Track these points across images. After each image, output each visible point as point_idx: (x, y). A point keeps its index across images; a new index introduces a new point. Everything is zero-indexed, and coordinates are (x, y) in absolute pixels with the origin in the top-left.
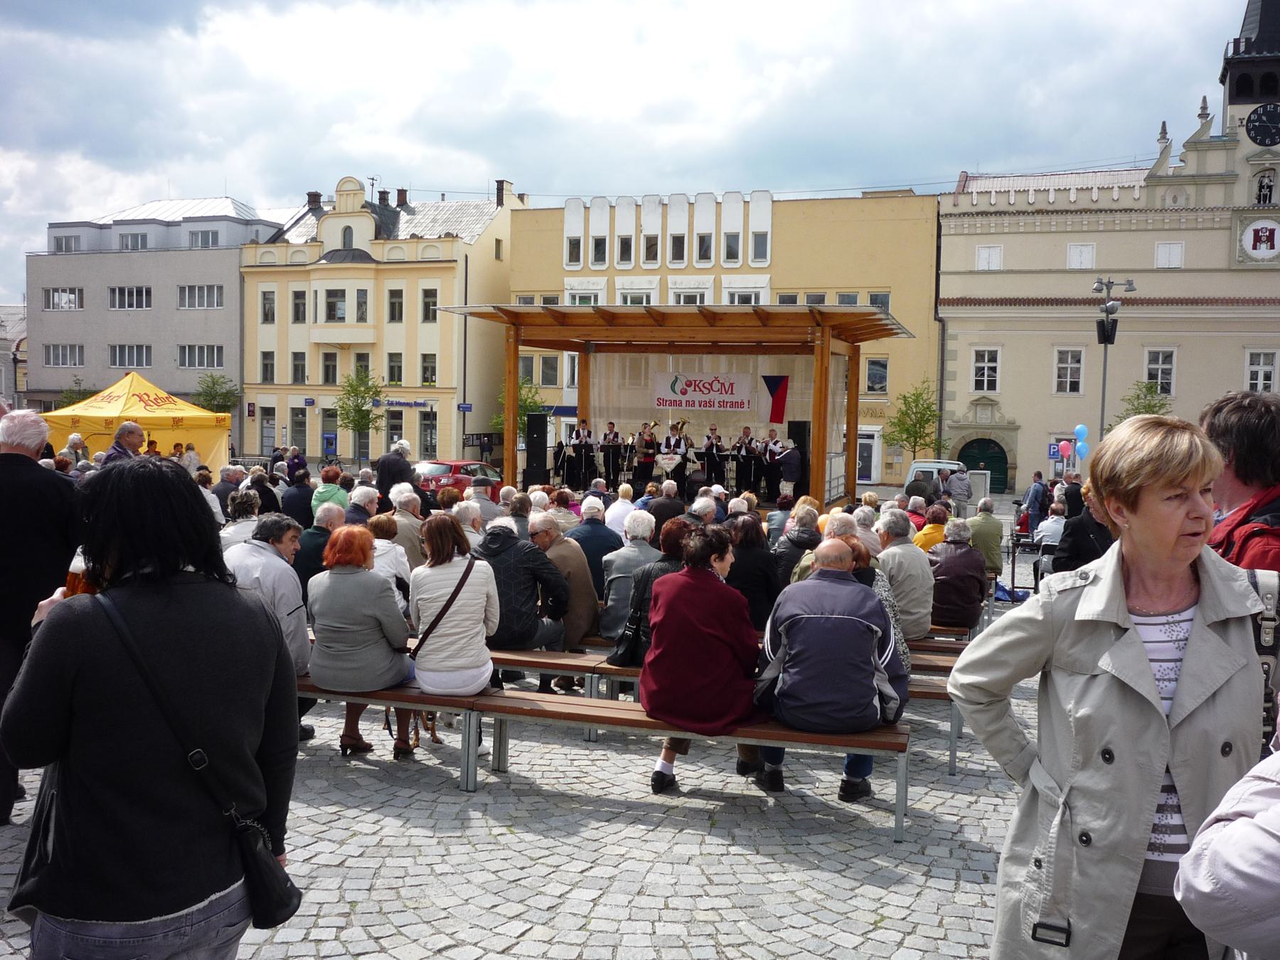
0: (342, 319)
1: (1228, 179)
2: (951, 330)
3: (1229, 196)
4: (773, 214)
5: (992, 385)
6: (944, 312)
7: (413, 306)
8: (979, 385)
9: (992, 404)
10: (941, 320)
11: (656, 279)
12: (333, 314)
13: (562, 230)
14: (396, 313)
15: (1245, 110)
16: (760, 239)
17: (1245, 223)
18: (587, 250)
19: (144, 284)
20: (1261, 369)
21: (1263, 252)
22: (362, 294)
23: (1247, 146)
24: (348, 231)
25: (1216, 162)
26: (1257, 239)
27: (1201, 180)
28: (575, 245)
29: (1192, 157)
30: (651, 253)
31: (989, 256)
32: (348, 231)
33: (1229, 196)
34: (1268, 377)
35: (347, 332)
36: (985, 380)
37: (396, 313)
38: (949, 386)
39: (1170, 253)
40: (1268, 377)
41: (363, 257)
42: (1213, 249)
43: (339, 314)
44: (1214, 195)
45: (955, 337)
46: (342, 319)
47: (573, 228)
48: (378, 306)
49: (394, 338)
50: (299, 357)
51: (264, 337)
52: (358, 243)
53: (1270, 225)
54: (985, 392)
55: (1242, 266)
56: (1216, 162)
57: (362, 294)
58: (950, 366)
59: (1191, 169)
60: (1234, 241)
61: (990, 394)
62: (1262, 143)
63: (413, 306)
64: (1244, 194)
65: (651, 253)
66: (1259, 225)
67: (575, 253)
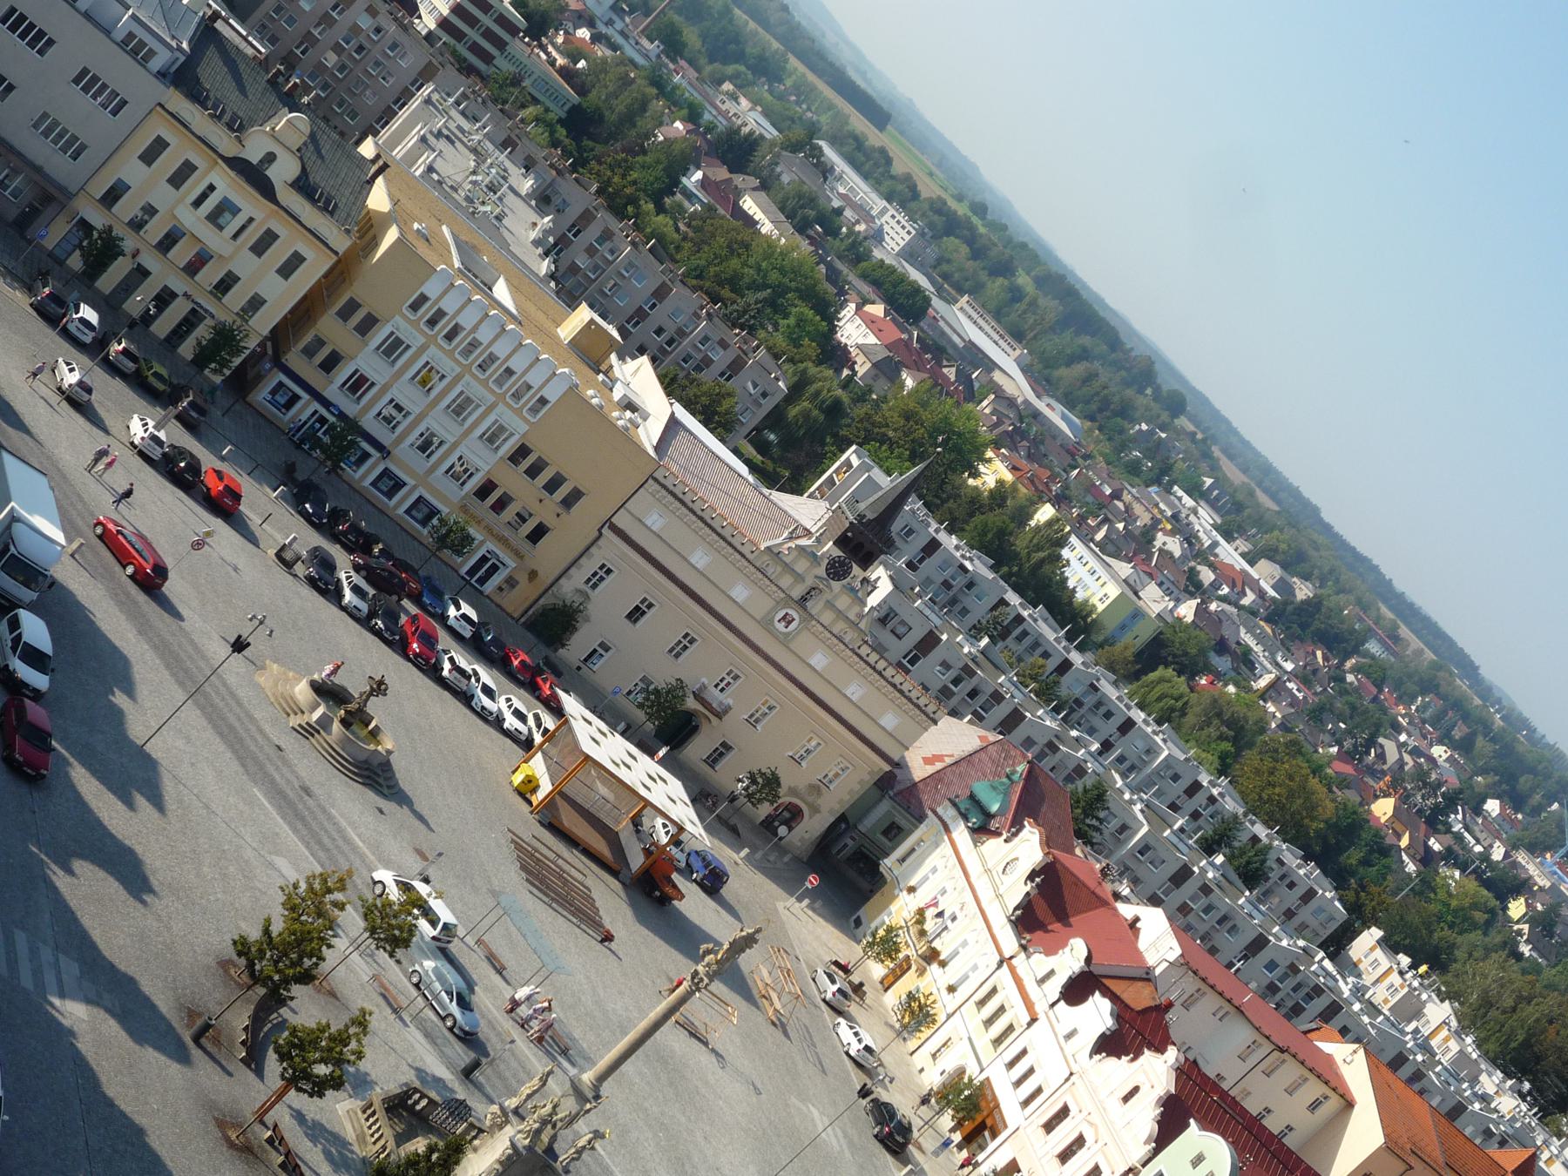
0: (221, 228)
1: (799, 578)
2: (600, 543)
3: (792, 586)
4: (565, 394)
5: (595, 586)
6: (605, 531)
7: (278, 254)
9: (587, 597)
10: (601, 534)
11: (458, 370)
12: (214, 217)
13: (423, 283)
14: (260, 248)
15: (837, 553)
16: (543, 401)
18: (426, 311)
19: (51, 33)
20: (728, 679)
21: (781, 626)
22: (251, 220)
23: (821, 571)
24: (270, 158)
25: (802, 566)
26: (784, 618)
27: (788, 568)
28: (423, 299)
29: (795, 553)
30: (467, 352)
31: (655, 520)
32: (270, 158)
33: (792, 586)
34: (729, 683)
35: (215, 241)
36: (595, 580)
37: (260, 248)
38: (573, 571)
39: (740, 592)
40: (729, 683)
41: (266, 189)
42: (762, 606)
43: (221, 221)
44: (785, 582)
45: (600, 548)
46: (221, 228)
47: (432, 289)
48: (253, 235)
49: (244, 264)
50: (150, 211)
51: (131, 170)
52: (272, 172)
53: (795, 615)
54: (587, 588)
55: (766, 624)
56: (802, 566)
57: (251, 220)
58: (583, 561)
59: (788, 560)
60: (774, 610)
61: (589, 591)
62: (828, 575)
63: (278, 254)
64: (797, 593)
65: (467, 352)
66: (790, 612)
67: (415, 307)
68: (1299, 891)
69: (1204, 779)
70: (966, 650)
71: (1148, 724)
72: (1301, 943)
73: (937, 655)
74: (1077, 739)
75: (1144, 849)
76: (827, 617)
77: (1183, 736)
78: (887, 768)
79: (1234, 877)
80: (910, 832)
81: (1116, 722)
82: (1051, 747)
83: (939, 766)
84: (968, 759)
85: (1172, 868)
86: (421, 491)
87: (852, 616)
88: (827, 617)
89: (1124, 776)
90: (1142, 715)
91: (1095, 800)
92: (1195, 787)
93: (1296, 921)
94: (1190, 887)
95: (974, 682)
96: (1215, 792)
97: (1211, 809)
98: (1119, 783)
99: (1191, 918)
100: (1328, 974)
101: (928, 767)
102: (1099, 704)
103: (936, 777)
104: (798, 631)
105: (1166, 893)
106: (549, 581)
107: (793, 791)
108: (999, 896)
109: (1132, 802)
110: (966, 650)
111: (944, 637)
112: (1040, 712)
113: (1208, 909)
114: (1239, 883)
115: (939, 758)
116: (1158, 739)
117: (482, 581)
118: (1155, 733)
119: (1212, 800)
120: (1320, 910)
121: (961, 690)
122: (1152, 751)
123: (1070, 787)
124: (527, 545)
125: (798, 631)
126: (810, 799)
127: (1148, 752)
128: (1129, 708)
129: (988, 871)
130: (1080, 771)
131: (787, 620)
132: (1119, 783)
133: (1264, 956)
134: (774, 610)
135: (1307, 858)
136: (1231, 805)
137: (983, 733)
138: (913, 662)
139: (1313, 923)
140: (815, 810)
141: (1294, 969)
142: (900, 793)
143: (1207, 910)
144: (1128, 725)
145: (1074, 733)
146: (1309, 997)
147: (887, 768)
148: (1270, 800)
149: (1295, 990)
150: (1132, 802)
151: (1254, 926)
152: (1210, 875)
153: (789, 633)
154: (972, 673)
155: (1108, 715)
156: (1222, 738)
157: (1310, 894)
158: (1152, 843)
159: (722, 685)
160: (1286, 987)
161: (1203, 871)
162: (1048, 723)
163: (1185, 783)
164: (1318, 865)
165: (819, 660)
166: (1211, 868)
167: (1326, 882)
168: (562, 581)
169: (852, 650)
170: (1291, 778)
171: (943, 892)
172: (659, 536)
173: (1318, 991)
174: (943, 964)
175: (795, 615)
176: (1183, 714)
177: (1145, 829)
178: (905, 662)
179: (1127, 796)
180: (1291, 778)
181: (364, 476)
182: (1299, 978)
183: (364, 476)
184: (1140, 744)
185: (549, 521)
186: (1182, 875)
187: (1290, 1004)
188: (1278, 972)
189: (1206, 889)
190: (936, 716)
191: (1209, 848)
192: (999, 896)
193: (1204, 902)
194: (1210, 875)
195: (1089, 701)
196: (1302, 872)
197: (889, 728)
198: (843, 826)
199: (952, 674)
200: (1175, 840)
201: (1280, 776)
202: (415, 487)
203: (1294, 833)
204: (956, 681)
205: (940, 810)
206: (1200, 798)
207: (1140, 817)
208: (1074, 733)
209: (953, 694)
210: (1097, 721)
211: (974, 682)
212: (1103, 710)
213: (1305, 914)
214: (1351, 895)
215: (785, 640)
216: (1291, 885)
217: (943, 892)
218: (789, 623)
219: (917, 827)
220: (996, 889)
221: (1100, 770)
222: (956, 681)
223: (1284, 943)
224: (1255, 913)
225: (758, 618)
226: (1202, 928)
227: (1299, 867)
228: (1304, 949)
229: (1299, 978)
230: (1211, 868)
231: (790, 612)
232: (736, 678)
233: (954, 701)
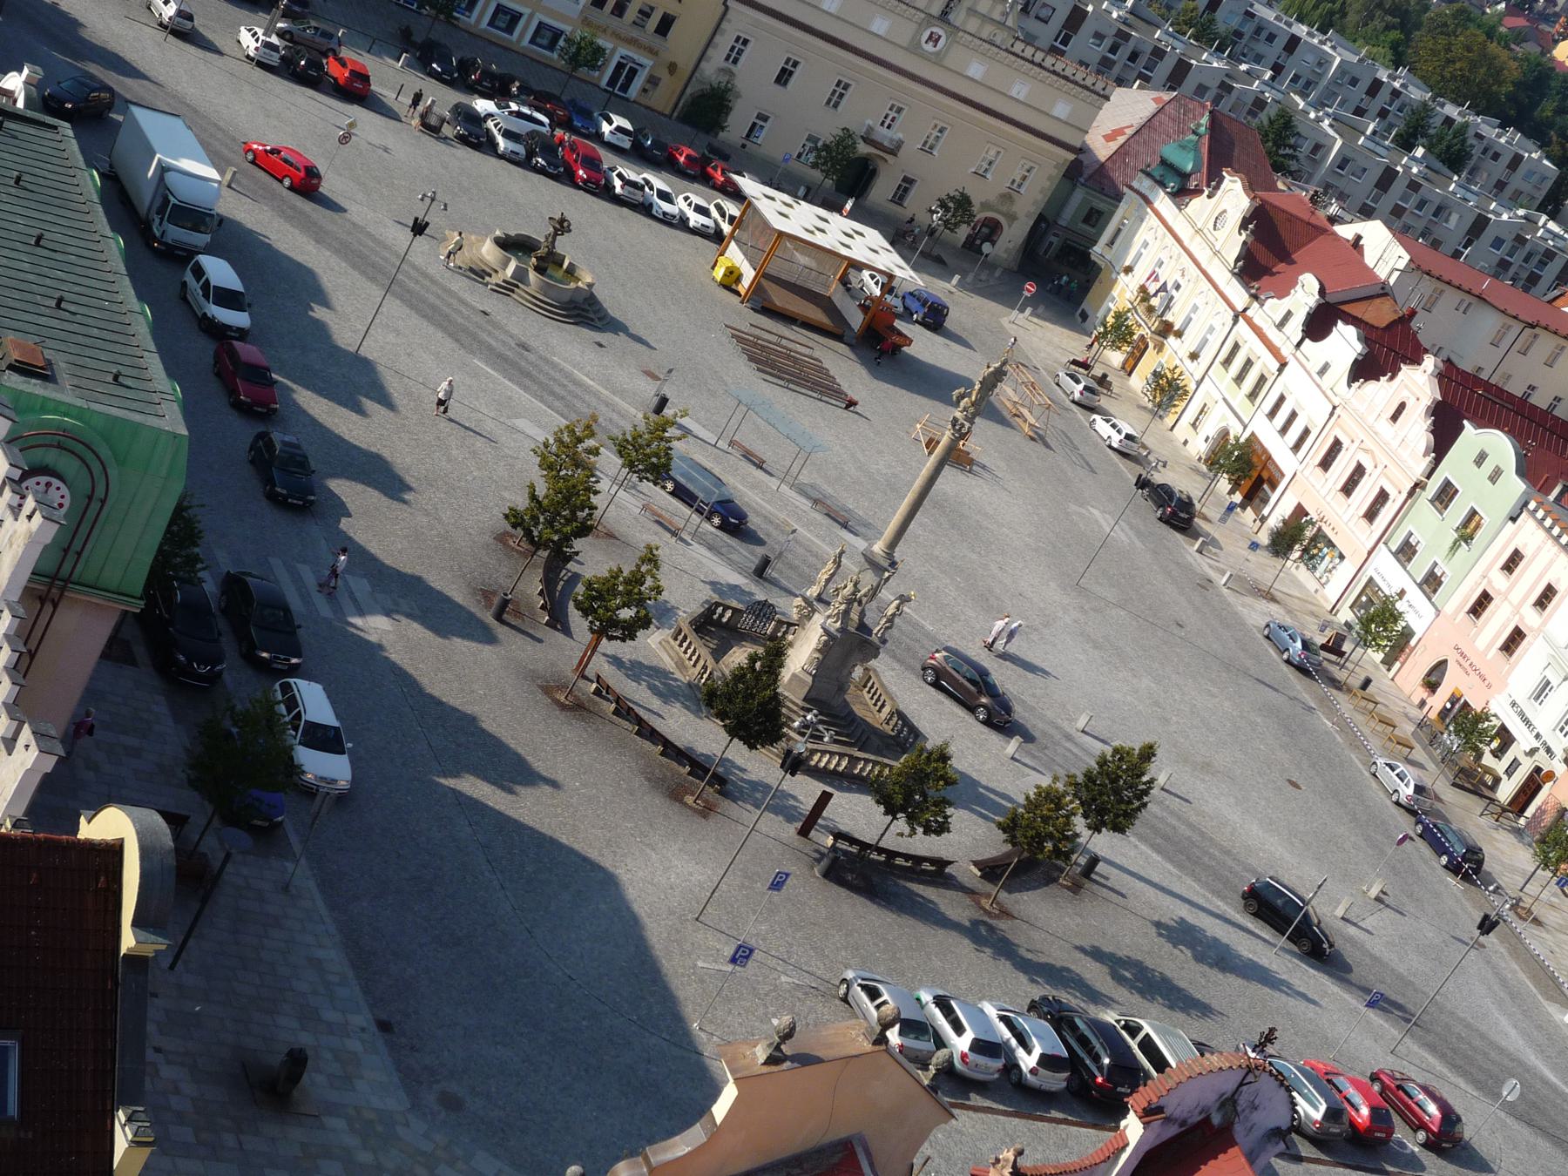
2: (728, 16)
5: (735, 61)
8: (727, 59)
9: (731, 74)
10: (727, 8)
17: (930, 25)
20: (892, 114)
21: (929, 47)
26: (930, 38)
34: (893, 119)
36: (734, 56)
38: (710, 52)
40: (893, 119)
42: (905, 31)
45: (729, 21)
53: (941, 32)
54: (729, 65)
55: (914, 48)
58: (718, 38)
60: (918, 33)
61: (732, 67)
66: (935, 30)
68: (1505, 160)
69: (1383, 75)
70: (1115, 15)
71: (1313, 36)
72: (1521, 212)
73: (1087, 28)
74: (1248, 72)
75: (1343, 162)
76: (973, 25)
77: (1350, 37)
78: (1072, 157)
79: (1438, 165)
80: (1112, 213)
81: (1280, 42)
82: (1226, 88)
83: (1121, 140)
84: (1149, 124)
85: (1374, 175)
86: (540, 17)
87: (996, 16)
88: (973, 25)
89: (1304, 96)
90: (1305, 28)
91: (1283, 129)
92: (1376, 86)
93: (1508, 191)
94: (1399, 187)
95: (1131, 45)
96: (1397, 85)
97: (1397, 103)
98: (1302, 104)
99: (1406, 218)
100: (1555, 236)
101: (1111, 144)
102: (1258, 31)
103: (1121, 152)
104: (948, 47)
105: (1376, 200)
106: (690, 68)
107: (985, 206)
108: (1216, 253)
109: (1318, 120)
110: (1115, 15)
111: (1090, 8)
112: (1205, 56)
113: (1421, 204)
114: (1445, 170)
115: (1120, 132)
116: (1327, 48)
117: (625, 88)
118: (1322, 42)
119: (1396, 93)
120: (1531, 173)
121: (1122, 56)
122: (1324, 62)
123: (1255, 122)
124: (657, 41)
125: (948, 47)
126: (1004, 209)
127: (1320, 64)
128: (1290, 25)
129: (1199, 231)
130: (1260, 103)
131: (933, 39)
132: (1302, 104)
133: (1488, 235)
134: (918, 33)
135: (1503, 126)
136: (1417, 94)
137: (1155, 94)
138: (1065, 42)
139: (1526, 187)
140: (1012, 218)
141: (1520, 240)
142: (1091, 177)
143: (1421, 204)
144: (1294, 41)
145: (1244, 67)
146: (1542, 264)
147: (1072, 157)
148: (1454, 77)
149: (1526, 260)
150: (1318, 120)
151: (1471, 209)
152: (1415, 170)
153: (941, 51)
154: (1127, 37)
155: (1271, 38)
156: (1388, 28)
157: (1517, 160)
158: (1350, 155)
159: (888, 121)
160: (1517, 260)
161: (1407, 168)
162: (1215, 65)
163: (1364, 85)
164: (1519, 129)
165: (976, 70)
166: (1414, 163)
167: (1529, 144)
168: (703, 64)
169: (1006, 50)
170: (1469, 50)
171: (1160, 264)
172: (838, 18)
173: (1549, 255)
174: (1179, 334)
175: (941, 32)
176: (1344, 15)
177: (1339, 143)
178: (1057, 44)
179: (1312, 115)
180: (1469, 50)
181: (479, 20)
182: (1528, 247)
183: (479, 20)
184: (1310, 58)
185: (673, 8)
186: (1387, 178)
187: (1525, 275)
188: (1506, 247)
189: (1414, 186)
190: (1107, 92)
191: (1406, 144)
192: (1216, 253)
193: (1414, 199)
194: (1415, 170)
195: (1248, 29)
196: (1503, 140)
197: (978, 77)
198: (1043, 225)
199: (1107, 43)
200: (1371, 145)
201: (1458, 50)
202: (531, 16)
203: (1485, 104)
204: (1114, 49)
205: (1135, 184)
206: (1384, 95)
207: (1331, 132)
208: (1244, 67)
209: (1114, 62)
210: (1261, 47)
211: (1131, 45)
212: (1264, 35)
213: (1516, 181)
214: (1556, 148)
215: (937, 60)
216: (1496, 156)
217: (1160, 264)
218: (937, 41)
219: (1117, 207)
220: (1211, 246)
221: (1279, 96)
222: (1114, 49)
223: (1505, 217)
224: (1469, 195)
225: (905, 45)
226: (1420, 225)
227: (1499, 136)
228: (1525, 217)
229: (1528, 247)
230: (1414, 163)
231: (935, 30)
232: (899, 110)
233: (1116, 70)
